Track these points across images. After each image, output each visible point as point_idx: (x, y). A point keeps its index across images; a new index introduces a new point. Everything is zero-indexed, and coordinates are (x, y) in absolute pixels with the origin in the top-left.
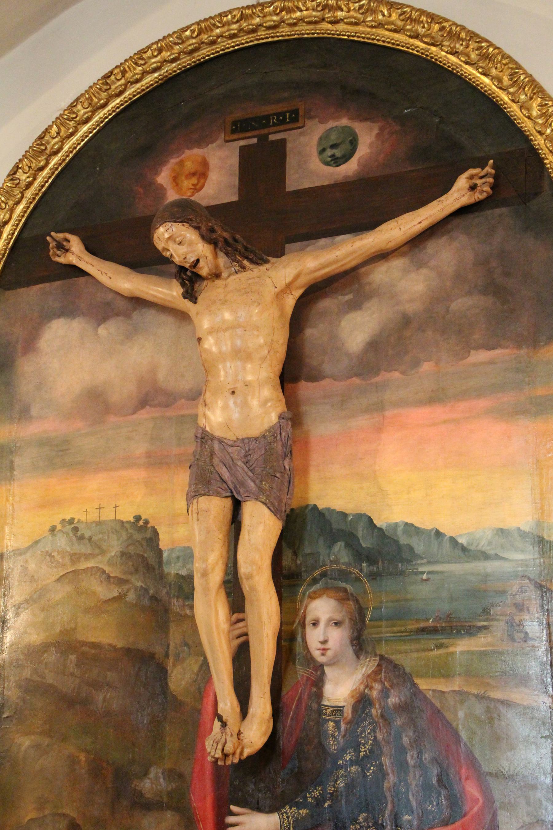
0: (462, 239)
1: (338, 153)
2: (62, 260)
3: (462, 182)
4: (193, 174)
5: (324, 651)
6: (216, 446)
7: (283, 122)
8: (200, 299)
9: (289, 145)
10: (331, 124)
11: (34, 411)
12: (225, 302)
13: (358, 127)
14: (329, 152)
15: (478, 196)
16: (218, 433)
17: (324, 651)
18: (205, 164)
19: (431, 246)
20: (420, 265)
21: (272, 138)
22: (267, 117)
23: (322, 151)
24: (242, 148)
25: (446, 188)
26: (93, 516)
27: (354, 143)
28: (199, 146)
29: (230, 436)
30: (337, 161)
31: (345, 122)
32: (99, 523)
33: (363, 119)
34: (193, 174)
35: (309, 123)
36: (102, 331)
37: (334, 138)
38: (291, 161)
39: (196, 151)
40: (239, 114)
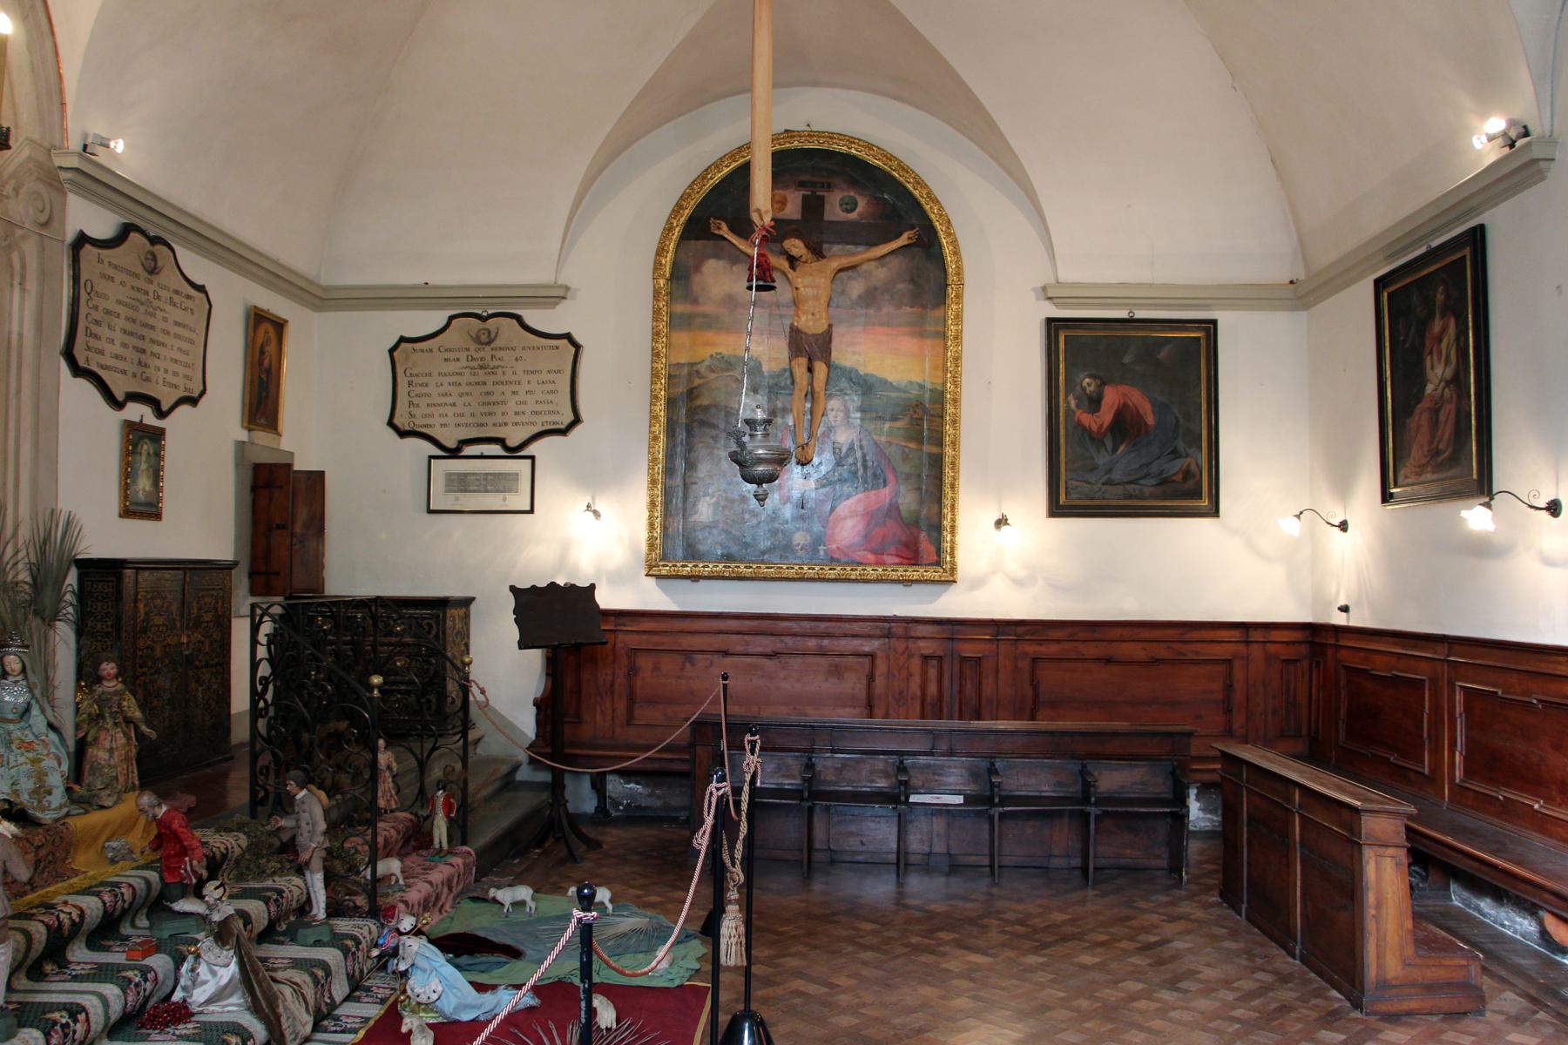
0: (901, 258)
1: (848, 207)
2: (716, 232)
3: (906, 235)
4: (779, 202)
5: (836, 421)
6: (803, 336)
7: (823, 187)
8: (798, 270)
9: (826, 199)
10: (846, 194)
11: (701, 300)
12: (811, 275)
13: (857, 197)
14: (844, 206)
15: (911, 242)
16: (804, 330)
17: (836, 421)
18: (785, 198)
19: (888, 259)
20: (883, 266)
21: (818, 193)
22: (816, 183)
23: (841, 205)
24: (804, 197)
25: (898, 236)
26: (731, 352)
27: (856, 205)
28: (782, 188)
29: (810, 332)
30: (849, 211)
31: (852, 194)
32: (735, 356)
33: (861, 194)
34: (779, 202)
35: (836, 191)
36: (735, 268)
37: (846, 200)
38: (827, 207)
39: (781, 192)
40: (803, 178)
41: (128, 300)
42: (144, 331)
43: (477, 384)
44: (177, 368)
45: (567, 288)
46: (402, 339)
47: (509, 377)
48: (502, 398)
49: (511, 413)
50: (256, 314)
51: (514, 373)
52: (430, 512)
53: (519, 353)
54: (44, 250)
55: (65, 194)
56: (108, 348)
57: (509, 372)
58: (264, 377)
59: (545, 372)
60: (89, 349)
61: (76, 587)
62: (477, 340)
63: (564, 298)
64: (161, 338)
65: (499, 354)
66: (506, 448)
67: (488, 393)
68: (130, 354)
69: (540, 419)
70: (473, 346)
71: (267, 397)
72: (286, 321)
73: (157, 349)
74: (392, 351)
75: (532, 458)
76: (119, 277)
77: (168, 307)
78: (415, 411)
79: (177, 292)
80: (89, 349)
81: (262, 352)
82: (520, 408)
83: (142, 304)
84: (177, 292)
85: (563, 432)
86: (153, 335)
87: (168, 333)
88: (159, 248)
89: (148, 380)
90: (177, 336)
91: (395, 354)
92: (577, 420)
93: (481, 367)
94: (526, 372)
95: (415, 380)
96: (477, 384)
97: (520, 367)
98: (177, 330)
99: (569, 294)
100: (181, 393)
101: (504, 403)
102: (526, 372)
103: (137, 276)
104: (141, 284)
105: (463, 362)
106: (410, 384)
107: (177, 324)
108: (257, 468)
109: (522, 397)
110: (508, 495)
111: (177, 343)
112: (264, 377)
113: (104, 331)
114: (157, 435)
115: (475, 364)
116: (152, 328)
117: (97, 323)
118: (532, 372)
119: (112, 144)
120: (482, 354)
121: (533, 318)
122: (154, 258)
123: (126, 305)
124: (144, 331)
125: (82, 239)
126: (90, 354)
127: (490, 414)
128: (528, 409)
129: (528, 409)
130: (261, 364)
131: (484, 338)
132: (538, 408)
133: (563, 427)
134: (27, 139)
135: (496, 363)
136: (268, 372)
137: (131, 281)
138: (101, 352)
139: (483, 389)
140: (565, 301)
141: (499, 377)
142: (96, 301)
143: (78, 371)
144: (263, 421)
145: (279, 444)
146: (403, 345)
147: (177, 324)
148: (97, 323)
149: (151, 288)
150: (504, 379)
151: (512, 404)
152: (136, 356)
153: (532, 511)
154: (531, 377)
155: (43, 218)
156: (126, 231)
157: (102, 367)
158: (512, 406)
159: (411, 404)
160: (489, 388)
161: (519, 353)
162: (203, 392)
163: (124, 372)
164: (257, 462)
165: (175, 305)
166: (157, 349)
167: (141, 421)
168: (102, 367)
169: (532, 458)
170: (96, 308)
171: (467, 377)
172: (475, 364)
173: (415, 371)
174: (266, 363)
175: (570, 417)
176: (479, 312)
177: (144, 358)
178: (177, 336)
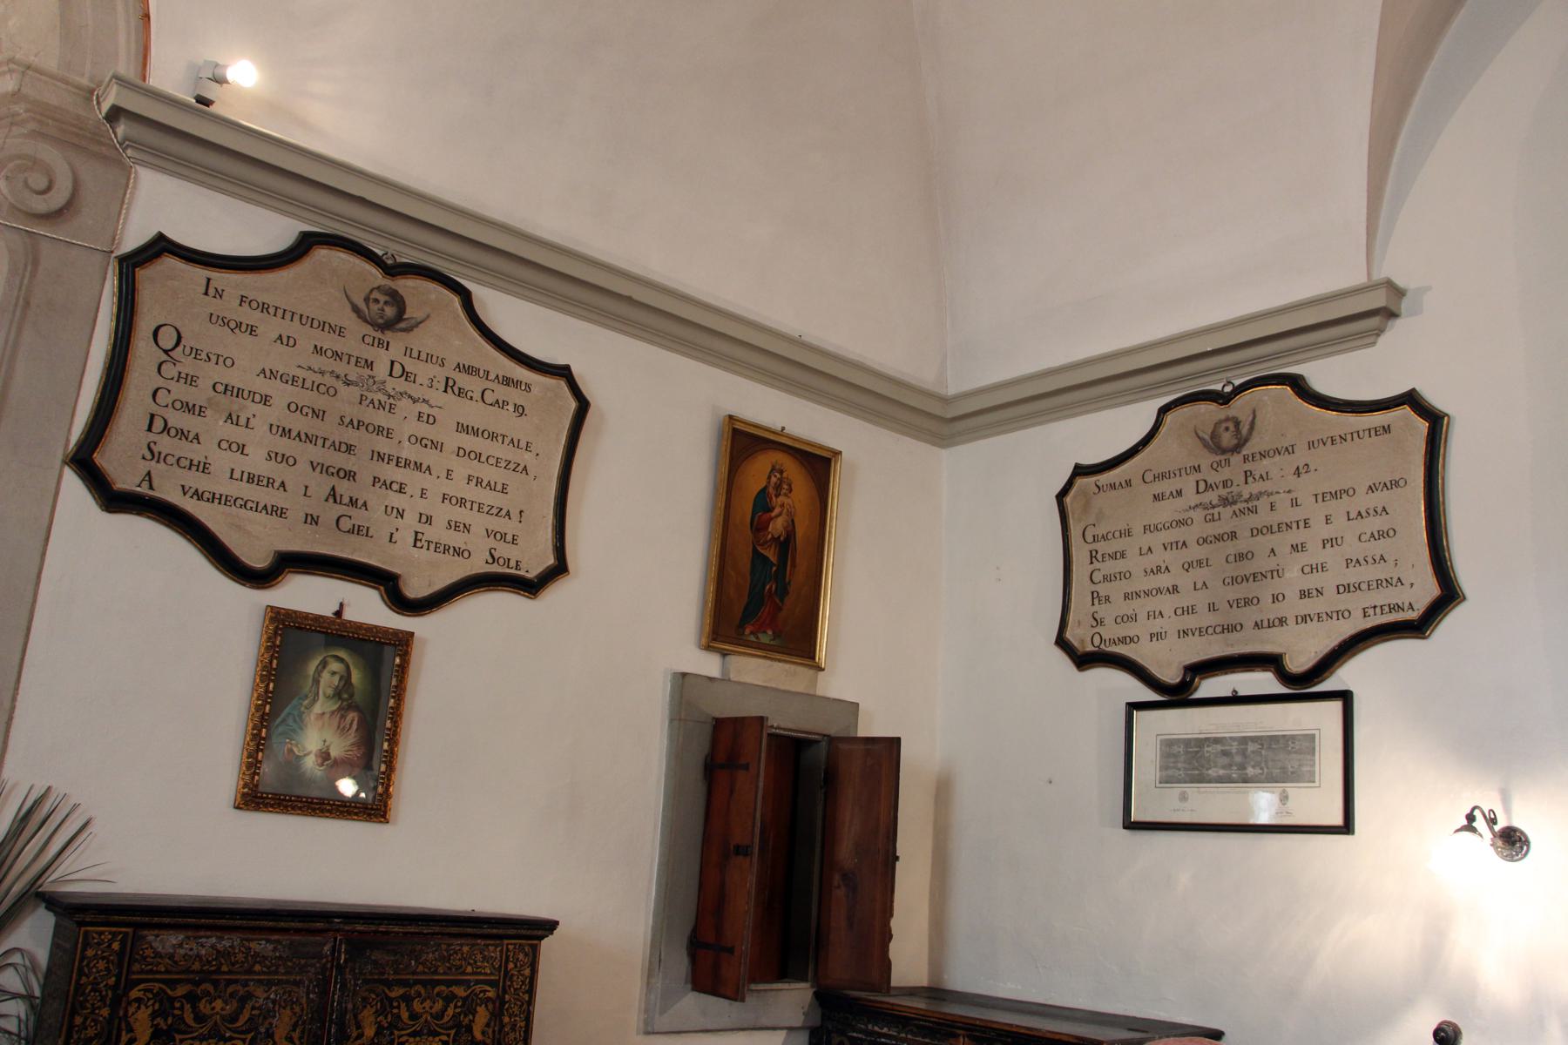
41: (301, 373)
42: (350, 436)
43: (1219, 538)
44: (462, 515)
45: (1399, 293)
46: (1080, 471)
47: (1286, 514)
48: (1271, 564)
49: (1292, 594)
50: (736, 433)
51: (1295, 503)
52: (1131, 825)
53: (1301, 457)
54: (36, 263)
55: (127, 172)
56: (222, 461)
57: (1282, 501)
58: (771, 554)
59: (1361, 490)
60: (154, 455)
61: (43, 956)
62: (1213, 444)
63: (1390, 314)
64: (409, 452)
65: (1260, 467)
66: (1285, 677)
67: (1241, 557)
68: (296, 476)
69: (1356, 602)
70: (1206, 459)
71: (783, 591)
72: (838, 453)
73: (390, 472)
74: (1061, 496)
75: (1345, 697)
76: (270, 327)
77: (437, 396)
78: (1102, 610)
79: (470, 370)
80: (154, 455)
81: (763, 503)
82: (1312, 582)
83: (348, 383)
84: (470, 370)
85: (1418, 627)
86: (383, 445)
87: (437, 446)
88: (408, 286)
89: (356, 530)
90: (461, 452)
91: (1068, 500)
92: (1449, 595)
93: (1225, 502)
94: (1323, 497)
95: (1102, 547)
96: (1219, 538)
97: (1305, 488)
98: (469, 442)
99: (1405, 305)
100: (478, 565)
101: (1276, 573)
102: (1323, 497)
103: (340, 332)
104: (351, 344)
105: (1191, 498)
106: (1093, 556)
107: (463, 428)
108: (719, 724)
109: (1315, 555)
110: (1293, 790)
111: (462, 468)
112: (771, 554)
113: (214, 427)
114: (403, 642)
115: (1212, 496)
116: (387, 433)
117: (189, 408)
118: (1336, 495)
119: (231, 74)
120: (1225, 473)
121: (1326, 375)
122: (396, 299)
123: (283, 378)
124: (350, 436)
125: (160, 247)
126: (158, 469)
127: (1248, 602)
128: (1328, 581)
129: (1328, 581)
130: (759, 526)
131: (1227, 439)
132: (1353, 575)
133: (1413, 615)
134: (11, 60)
135: (1254, 487)
136: (786, 544)
137: (308, 338)
138: (204, 467)
139: (1231, 548)
140: (1396, 329)
141: (1263, 517)
142: (188, 366)
143: (114, 500)
144: (765, 639)
145: (815, 684)
146: (1081, 482)
147: (463, 428)
148: (189, 408)
149: (382, 360)
150: (1274, 519)
151: (1292, 573)
152: (320, 485)
153: (1347, 827)
154: (1334, 506)
155: (41, 205)
156: (305, 245)
157: (198, 495)
158: (1293, 579)
159: (1095, 596)
160: (1242, 545)
161: (1301, 457)
162: (560, 568)
163: (281, 512)
164: (718, 715)
165: (461, 393)
166: (390, 472)
167: (339, 614)
168: (198, 495)
169: (1345, 697)
170: (191, 380)
171: (1199, 528)
172: (1212, 496)
173: (1101, 530)
174: (777, 526)
175: (1426, 590)
176: (1218, 387)
177: (344, 488)
178: (461, 452)
